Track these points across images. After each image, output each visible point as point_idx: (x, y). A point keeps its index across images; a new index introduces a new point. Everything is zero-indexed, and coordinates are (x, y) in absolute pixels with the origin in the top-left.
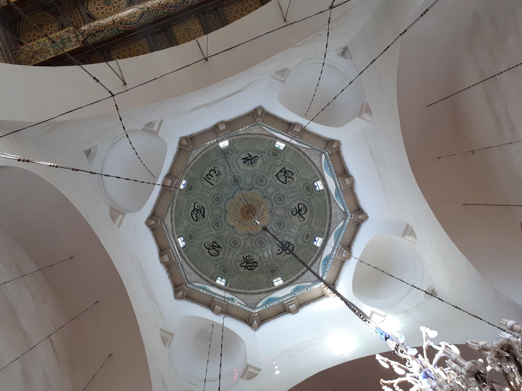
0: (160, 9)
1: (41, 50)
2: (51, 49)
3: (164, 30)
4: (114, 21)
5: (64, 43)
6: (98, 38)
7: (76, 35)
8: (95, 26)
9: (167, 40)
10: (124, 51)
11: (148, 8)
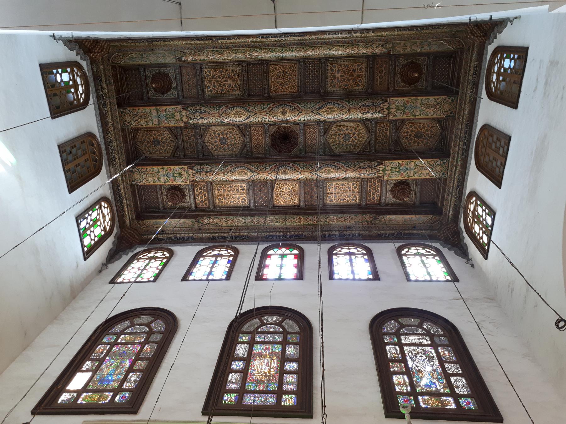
0: (301, 108)
1: (427, 108)
2: (418, 105)
3: (306, 93)
4: (349, 111)
5: (404, 106)
6: (371, 101)
7: (389, 110)
8: (369, 112)
9: (307, 82)
10: (352, 86)
11: (312, 112)
